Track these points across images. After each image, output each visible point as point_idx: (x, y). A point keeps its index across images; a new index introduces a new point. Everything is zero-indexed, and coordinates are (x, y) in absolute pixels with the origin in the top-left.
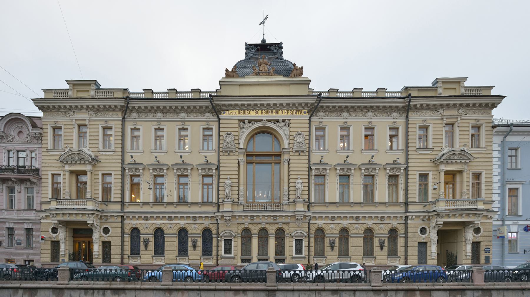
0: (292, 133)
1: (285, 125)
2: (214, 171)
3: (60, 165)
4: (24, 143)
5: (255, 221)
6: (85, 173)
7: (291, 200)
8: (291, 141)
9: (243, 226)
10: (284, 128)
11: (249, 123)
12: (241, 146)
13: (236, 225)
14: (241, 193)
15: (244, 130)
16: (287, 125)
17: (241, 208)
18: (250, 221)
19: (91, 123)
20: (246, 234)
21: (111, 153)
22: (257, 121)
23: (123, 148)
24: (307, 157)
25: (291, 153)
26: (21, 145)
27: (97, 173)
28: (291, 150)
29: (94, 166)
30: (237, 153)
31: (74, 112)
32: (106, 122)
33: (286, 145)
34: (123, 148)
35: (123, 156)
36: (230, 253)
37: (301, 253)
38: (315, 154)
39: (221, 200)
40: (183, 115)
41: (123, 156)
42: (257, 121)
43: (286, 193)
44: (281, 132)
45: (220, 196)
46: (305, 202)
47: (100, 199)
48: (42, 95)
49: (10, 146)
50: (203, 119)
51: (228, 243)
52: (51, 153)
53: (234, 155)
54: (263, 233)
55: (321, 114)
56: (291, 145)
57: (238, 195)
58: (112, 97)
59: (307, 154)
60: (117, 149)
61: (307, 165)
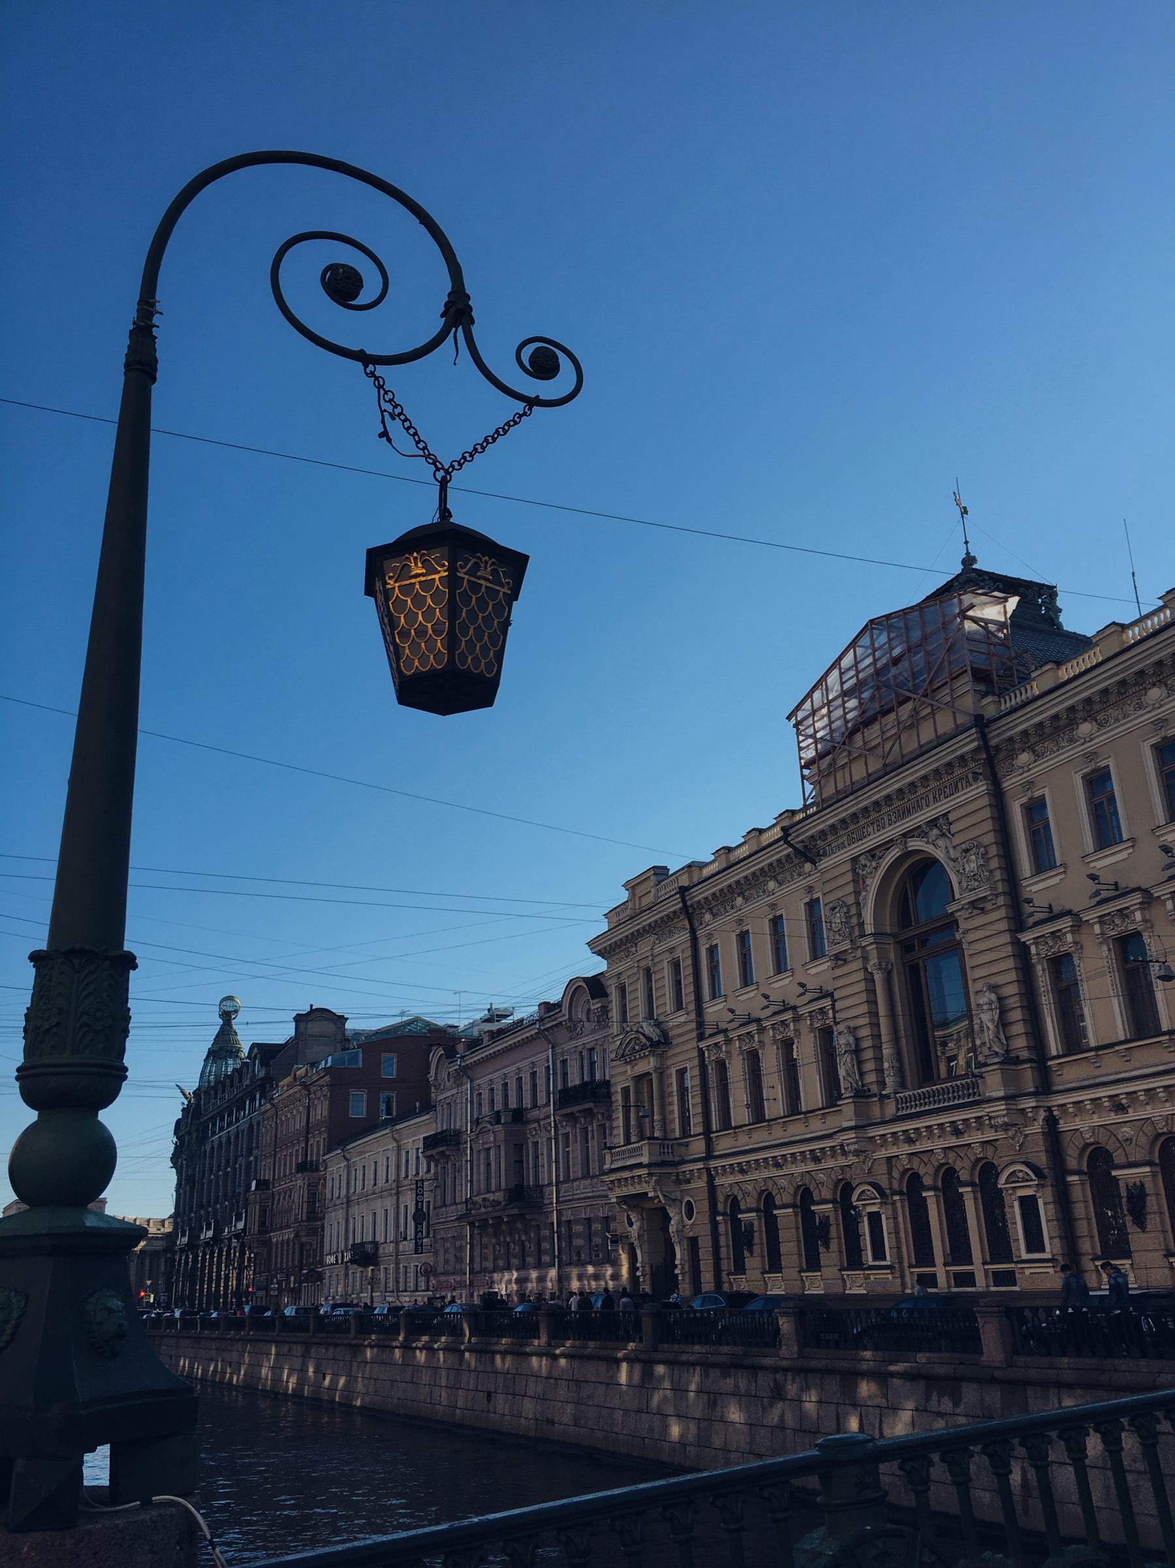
4: (593, 1031)
5: (918, 1147)
10: (941, 843)
13: (882, 1169)
14: (886, 1065)
17: (890, 1110)
29: (662, 1056)
30: (859, 953)
37: (1042, 1249)
38: (1034, 888)
42: (887, 845)
46: (1018, 1061)
47: (677, 1135)
48: (604, 927)
57: (861, 1074)
61: (1006, 938)
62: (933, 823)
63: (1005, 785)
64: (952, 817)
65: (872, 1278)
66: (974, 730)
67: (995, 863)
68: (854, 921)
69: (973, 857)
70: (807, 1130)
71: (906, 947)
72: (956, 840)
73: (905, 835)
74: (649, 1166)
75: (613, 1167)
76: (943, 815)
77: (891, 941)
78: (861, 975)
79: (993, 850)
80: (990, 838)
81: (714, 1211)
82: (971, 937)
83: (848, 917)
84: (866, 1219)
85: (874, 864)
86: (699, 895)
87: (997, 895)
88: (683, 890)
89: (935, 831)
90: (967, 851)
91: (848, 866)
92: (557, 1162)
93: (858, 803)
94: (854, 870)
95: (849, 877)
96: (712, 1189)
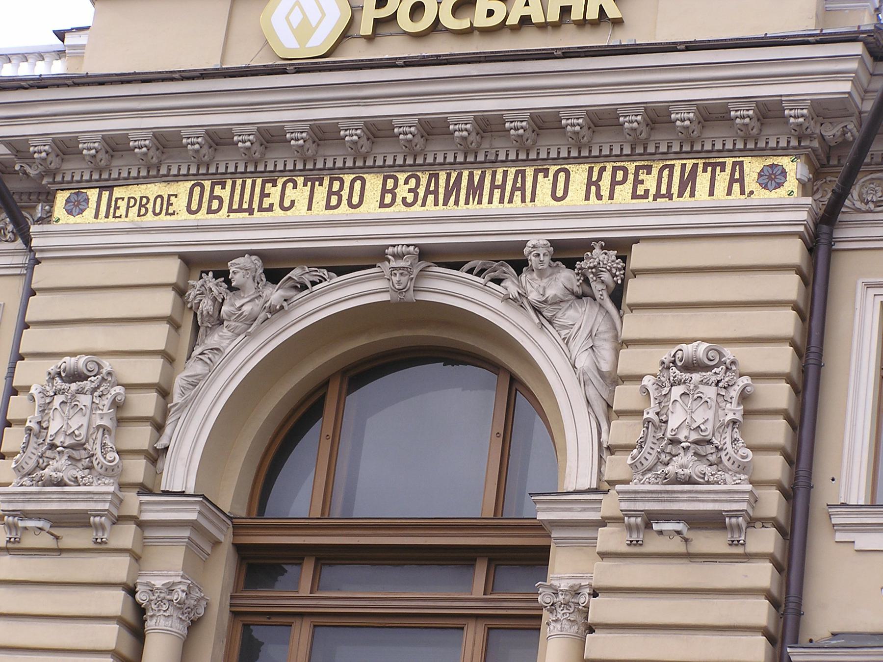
0: (631, 361)
8: (623, 431)
11: (274, 276)
24: (762, 575)
25: (611, 538)
28: (610, 505)
30: (126, 536)
38: (864, 541)
53: (101, 548)
56: (618, 467)
59: (767, 540)
62: (567, 253)
63: (839, 234)
64: (639, 257)
66: (857, 48)
67: (777, 431)
68: (140, 437)
69: (710, 392)
71: (258, 565)
72: (634, 326)
73: (425, 254)
76: (609, 245)
77: (226, 538)
78: (114, 602)
79: (779, 395)
80: (783, 359)
82: (602, 610)
83: (122, 417)
85: (275, 294)
87: (752, 522)
89: (565, 277)
90: (693, 366)
91: (171, 270)
94: (181, 291)
95: (164, 303)
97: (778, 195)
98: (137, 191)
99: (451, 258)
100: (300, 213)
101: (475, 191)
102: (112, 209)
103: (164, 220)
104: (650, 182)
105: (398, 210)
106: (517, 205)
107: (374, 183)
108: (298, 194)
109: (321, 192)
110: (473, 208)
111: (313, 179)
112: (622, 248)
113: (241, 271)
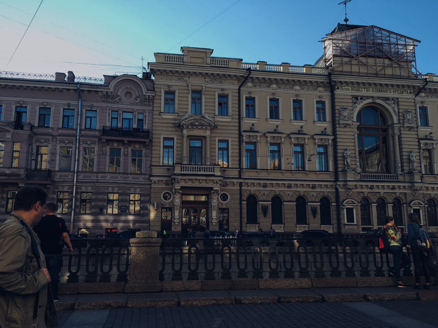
1: (394, 103)
2: (330, 141)
3: (174, 129)
4: (132, 104)
6: (202, 138)
7: (406, 172)
9: (362, 195)
11: (361, 99)
12: (355, 120)
15: (356, 105)
16: (395, 103)
18: (369, 190)
19: (207, 89)
20: (366, 204)
21: (229, 120)
22: (368, 97)
23: (239, 115)
26: (129, 107)
27: (213, 139)
31: (189, 77)
32: (222, 90)
33: (396, 121)
34: (239, 115)
35: (239, 123)
36: (354, 222)
38: (421, 129)
39: (340, 169)
40: (297, 87)
41: (239, 123)
42: (368, 97)
43: (400, 165)
44: (389, 108)
45: (340, 166)
49: (115, 106)
50: (317, 93)
51: (350, 211)
52: (165, 117)
54: (382, 204)
55: (423, 94)
58: (228, 66)
60: (234, 117)
62: (393, 99)
65: (346, 228)
70: (306, 177)
74: (220, 176)
75: (182, 172)
81: (241, 200)
84: (345, 210)
86: (253, 75)
88: (249, 69)
91: (351, 97)
92: (78, 161)
93: (368, 80)
96: (240, 190)
97: (411, 95)
98: (345, 88)
99: (379, 98)
100: (363, 92)
101: (382, 91)
102: (342, 89)
103: (348, 91)
104: (399, 92)
105: (374, 93)
106: (386, 93)
107: (371, 89)
108: (363, 90)
109: (366, 90)
110: (382, 93)
111: (365, 88)
112: (398, 98)
113: (359, 98)
